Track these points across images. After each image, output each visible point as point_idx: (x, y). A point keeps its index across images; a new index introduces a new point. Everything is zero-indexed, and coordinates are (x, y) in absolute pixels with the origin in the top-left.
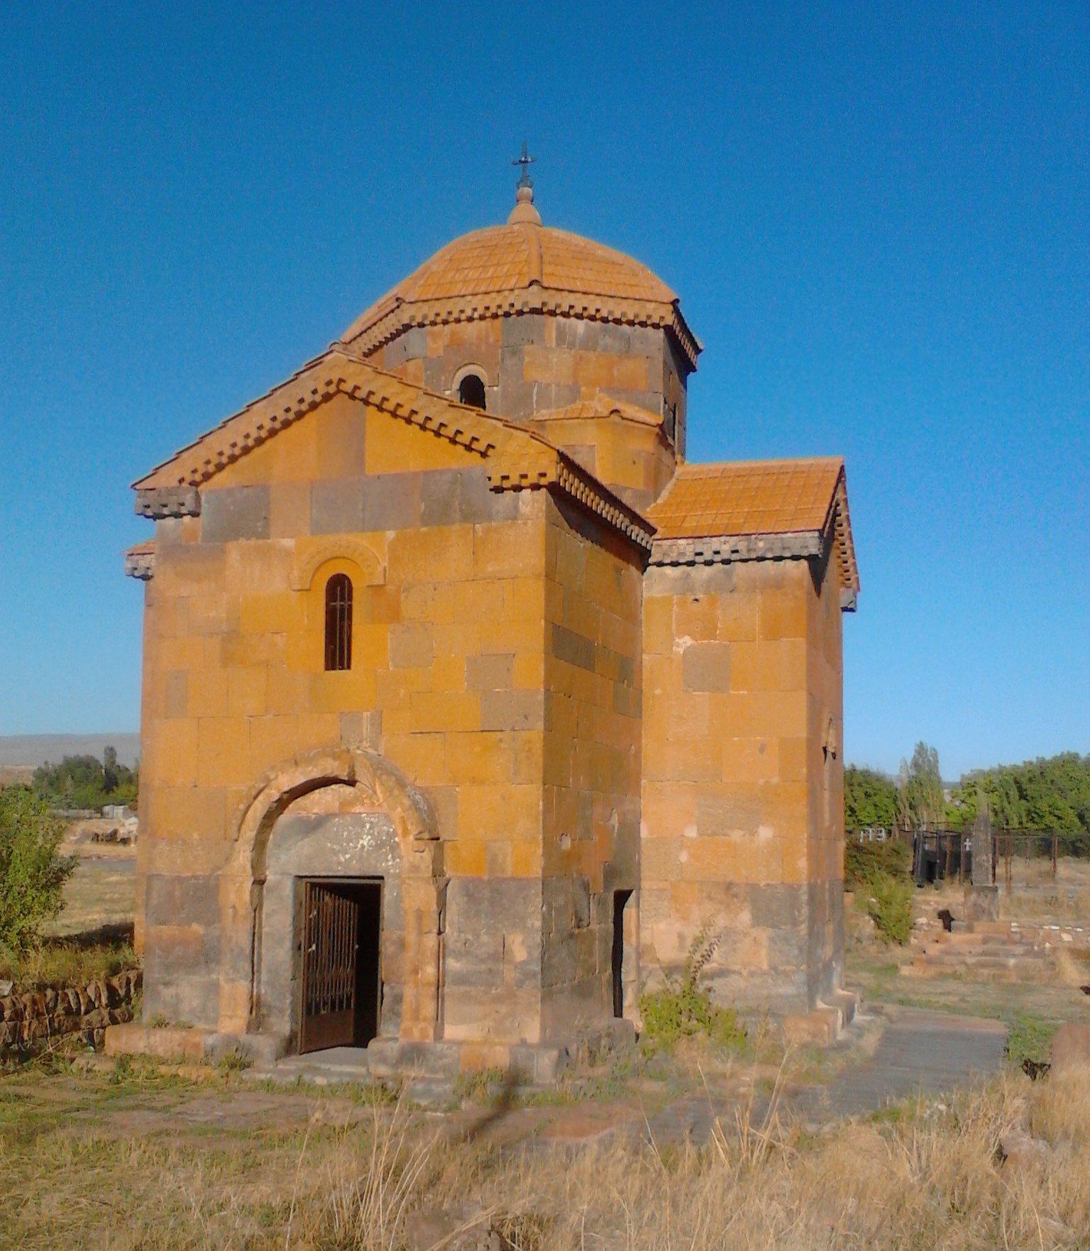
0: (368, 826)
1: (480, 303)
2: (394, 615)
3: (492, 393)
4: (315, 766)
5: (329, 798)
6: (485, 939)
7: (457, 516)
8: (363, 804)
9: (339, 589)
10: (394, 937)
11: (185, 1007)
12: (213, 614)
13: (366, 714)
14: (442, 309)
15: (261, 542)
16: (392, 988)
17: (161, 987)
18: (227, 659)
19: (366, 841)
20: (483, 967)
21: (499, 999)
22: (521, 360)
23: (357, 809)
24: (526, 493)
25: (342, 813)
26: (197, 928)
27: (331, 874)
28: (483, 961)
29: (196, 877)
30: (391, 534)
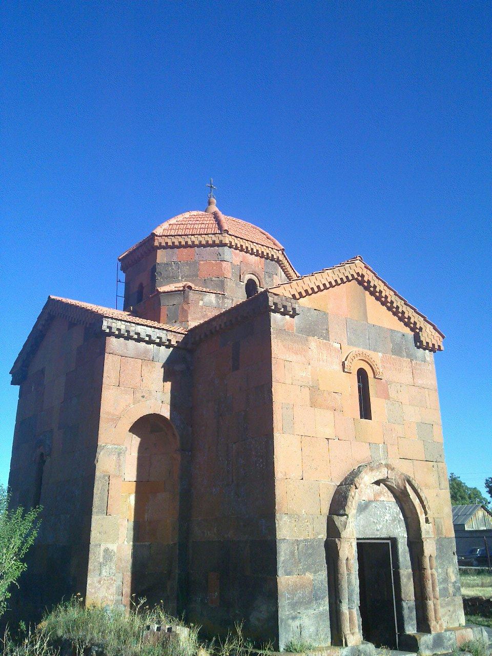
0: (388, 508)
1: (261, 249)
2: (387, 397)
4: (380, 472)
5: (369, 491)
6: (440, 570)
7: (405, 354)
8: (384, 496)
10: (406, 573)
11: (305, 634)
12: (304, 375)
13: (381, 445)
14: (245, 244)
15: (325, 341)
16: (407, 603)
17: (290, 621)
18: (313, 404)
19: (388, 517)
20: (441, 586)
21: (448, 604)
22: (272, 280)
23: (382, 498)
24: (427, 351)
25: (375, 500)
26: (309, 576)
27: (373, 537)
28: (441, 583)
29: (306, 540)
30: (380, 354)
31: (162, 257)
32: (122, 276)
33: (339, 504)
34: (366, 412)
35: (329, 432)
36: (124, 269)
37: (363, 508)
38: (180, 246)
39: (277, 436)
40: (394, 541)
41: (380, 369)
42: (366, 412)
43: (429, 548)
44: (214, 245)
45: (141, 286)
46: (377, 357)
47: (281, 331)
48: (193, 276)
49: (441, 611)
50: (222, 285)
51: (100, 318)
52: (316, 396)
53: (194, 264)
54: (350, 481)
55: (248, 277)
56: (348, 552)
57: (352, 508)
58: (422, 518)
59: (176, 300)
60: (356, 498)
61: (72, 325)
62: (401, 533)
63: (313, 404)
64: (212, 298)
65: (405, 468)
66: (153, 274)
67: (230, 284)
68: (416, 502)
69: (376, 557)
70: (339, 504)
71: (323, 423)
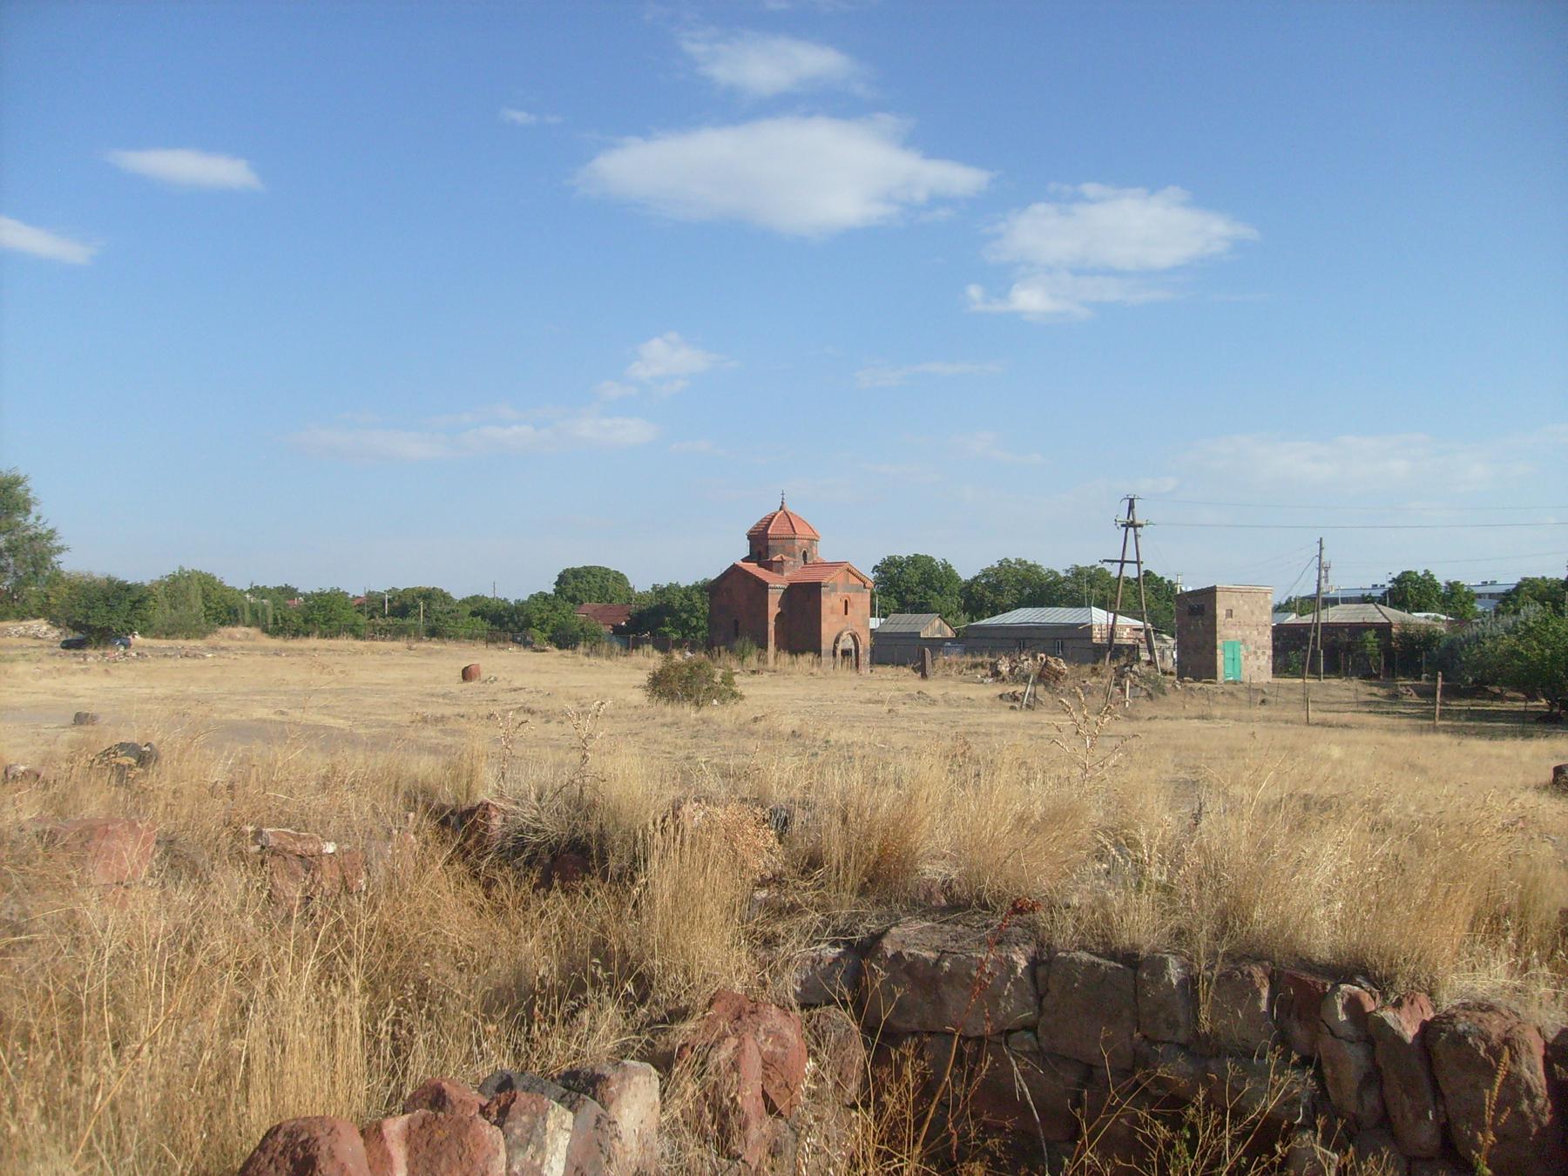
31: (770, 543)
33: (837, 641)
48: (783, 552)
54: (840, 634)
56: (839, 652)
66: (767, 548)
69: (846, 653)
70: (837, 641)
71: (834, 618)
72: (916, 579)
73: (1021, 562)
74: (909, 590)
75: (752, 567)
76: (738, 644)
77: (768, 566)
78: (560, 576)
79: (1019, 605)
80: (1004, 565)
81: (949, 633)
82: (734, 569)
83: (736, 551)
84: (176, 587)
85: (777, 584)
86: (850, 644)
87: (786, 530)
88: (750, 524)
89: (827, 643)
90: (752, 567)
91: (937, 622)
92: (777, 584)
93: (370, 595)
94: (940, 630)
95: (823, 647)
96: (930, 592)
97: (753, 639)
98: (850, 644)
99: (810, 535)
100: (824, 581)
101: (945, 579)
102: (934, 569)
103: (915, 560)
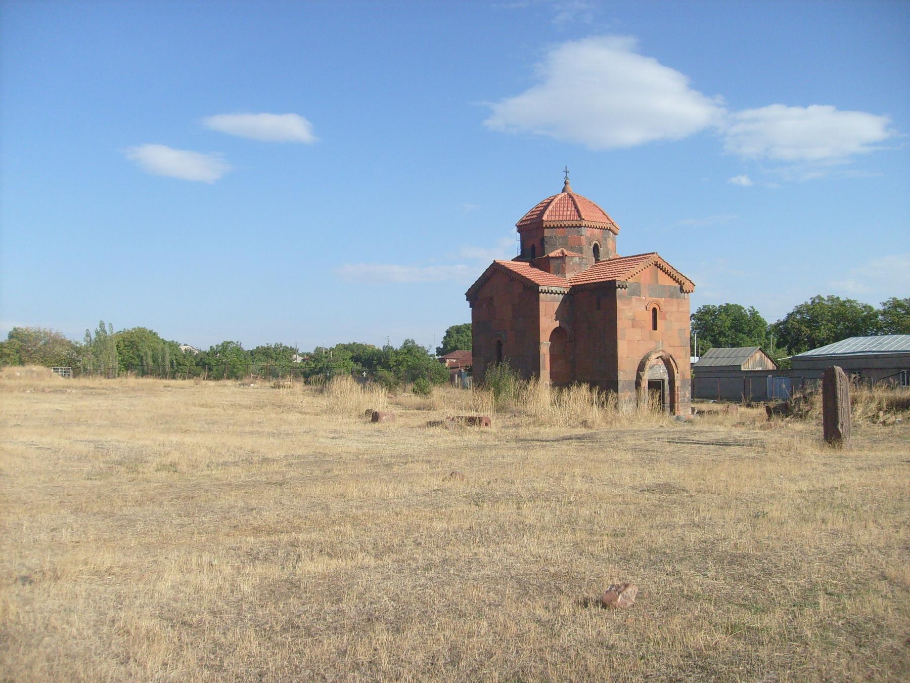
2: (664, 318)
3: (601, 249)
9: (654, 310)
14: (593, 224)
18: (633, 326)
31: (547, 233)
32: (519, 235)
33: (641, 367)
34: (655, 327)
35: (638, 337)
36: (519, 231)
37: (651, 368)
38: (558, 227)
39: (619, 341)
40: (663, 380)
41: (663, 307)
42: (655, 327)
43: (678, 383)
44: (576, 226)
45: (533, 247)
46: (662, 301)
47: (621, 296)
48: (565, 245)
49: (680, 408)
50: (580, 250)
51: (538, 285)
52: (635, 323)
53: (565, 238)
55: (594, 242)
56: (645, 384)
57: (647, 368)
58: (676, 371)
59: (559, 261)
60: (649, 364)
61: (511, 280)
62: (666, 377)
63: (633, 326)
64: (577, 259)
65: (670, 351)
66: (542, 241)
67: (585, 248)
68: (674, 365)
69: (655, 385)
70: (641, 367)
71: (637, 334)
72: (728, 324)
73: (831, 299)
74: (721, 333)
75: (525, 269)
76: (493, 373)
77: (544, 264)
78: (447, 332)
79: (837, 339)
80: (817, 302)
81: (770, 366)
82: (496, 270)
83: (506, 250)
84: (265, 353)
85: (552, 289)
86: (661, 373)
87: (568, 215)
88: (521, 212)
89: (626, 372)
90: (525, 269)
91: (758, 355)
92: (552, 289)
93: (318, 350)
94: (761, 363)
95: (621, 376)
96: (741, 335)
97: (514, 367)
98: (661, 373)
99: (600, 221)
100: (620, 279)
101: (752, 323)
102: (743, 316)
103: (727, 309)
